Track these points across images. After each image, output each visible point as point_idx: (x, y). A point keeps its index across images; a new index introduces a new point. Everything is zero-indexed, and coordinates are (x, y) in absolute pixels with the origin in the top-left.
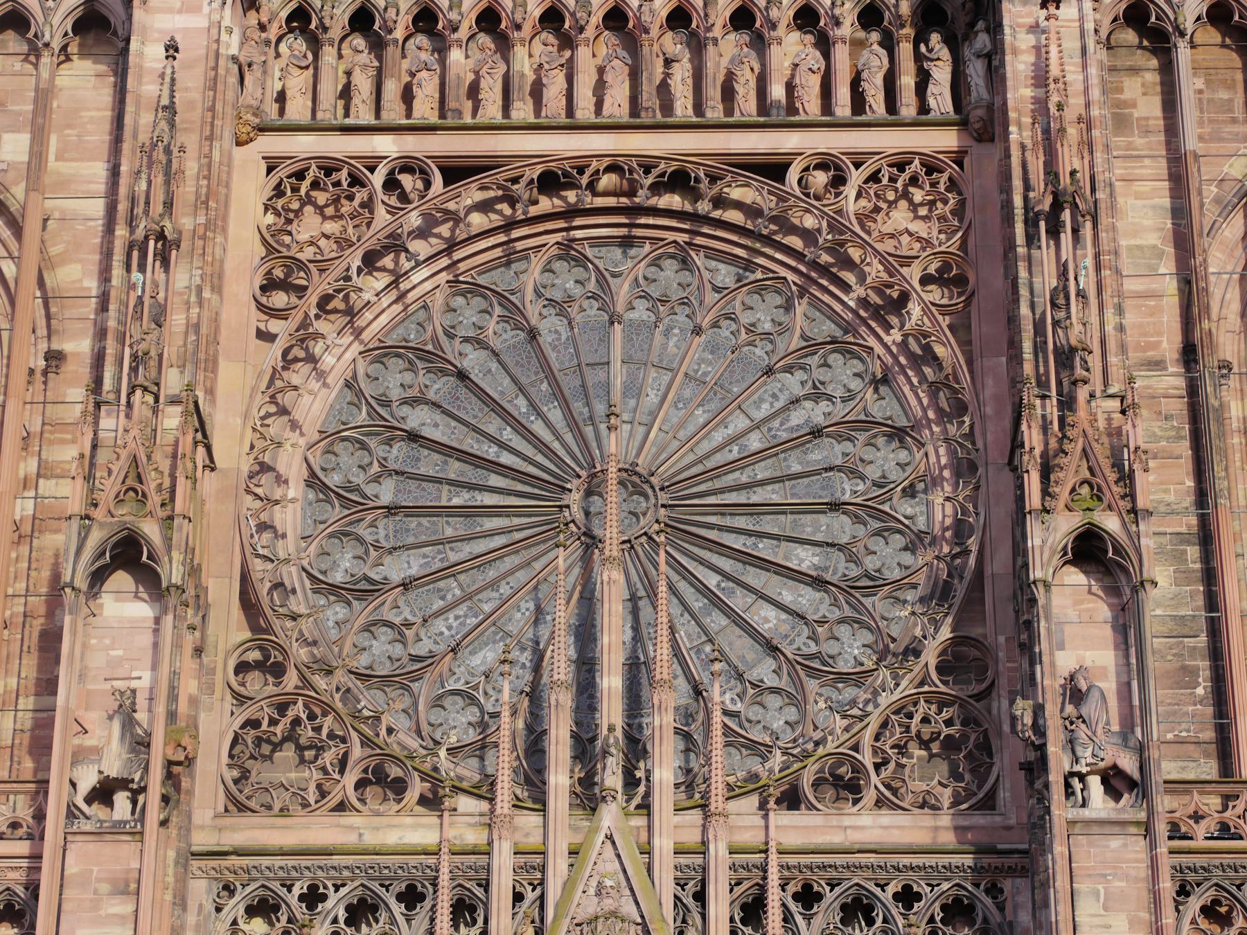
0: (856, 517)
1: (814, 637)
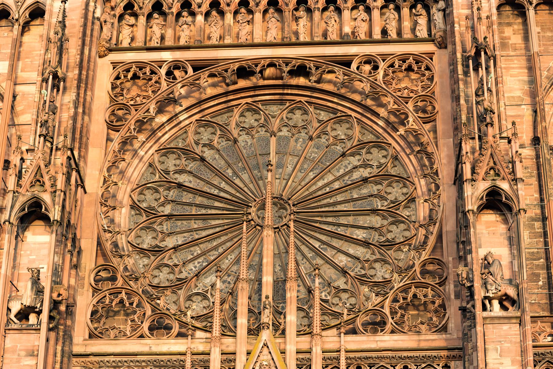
0: (383, 216)
1: (363, 268)
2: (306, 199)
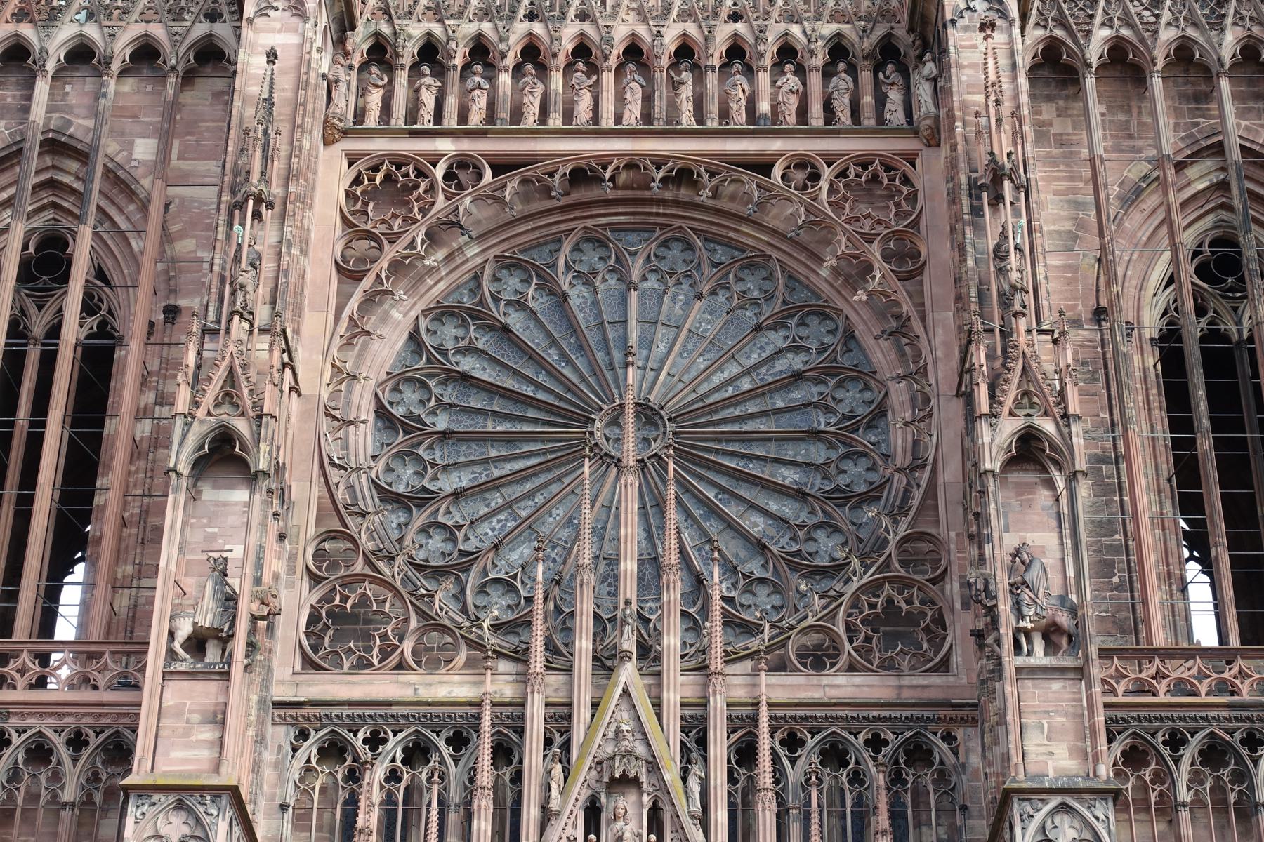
1: (794, 539)
2: (691, 408)
